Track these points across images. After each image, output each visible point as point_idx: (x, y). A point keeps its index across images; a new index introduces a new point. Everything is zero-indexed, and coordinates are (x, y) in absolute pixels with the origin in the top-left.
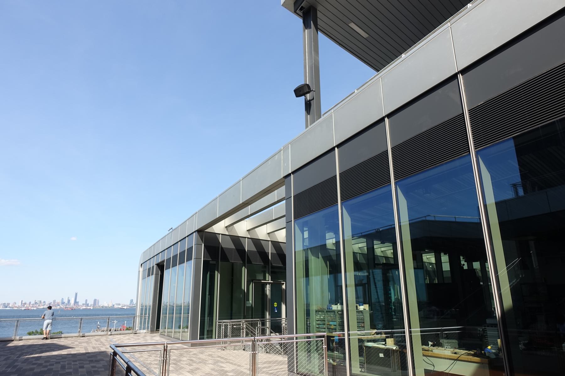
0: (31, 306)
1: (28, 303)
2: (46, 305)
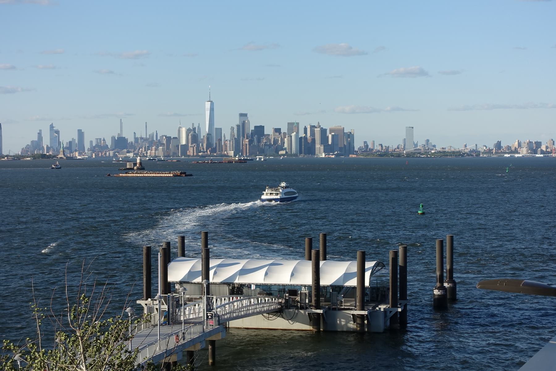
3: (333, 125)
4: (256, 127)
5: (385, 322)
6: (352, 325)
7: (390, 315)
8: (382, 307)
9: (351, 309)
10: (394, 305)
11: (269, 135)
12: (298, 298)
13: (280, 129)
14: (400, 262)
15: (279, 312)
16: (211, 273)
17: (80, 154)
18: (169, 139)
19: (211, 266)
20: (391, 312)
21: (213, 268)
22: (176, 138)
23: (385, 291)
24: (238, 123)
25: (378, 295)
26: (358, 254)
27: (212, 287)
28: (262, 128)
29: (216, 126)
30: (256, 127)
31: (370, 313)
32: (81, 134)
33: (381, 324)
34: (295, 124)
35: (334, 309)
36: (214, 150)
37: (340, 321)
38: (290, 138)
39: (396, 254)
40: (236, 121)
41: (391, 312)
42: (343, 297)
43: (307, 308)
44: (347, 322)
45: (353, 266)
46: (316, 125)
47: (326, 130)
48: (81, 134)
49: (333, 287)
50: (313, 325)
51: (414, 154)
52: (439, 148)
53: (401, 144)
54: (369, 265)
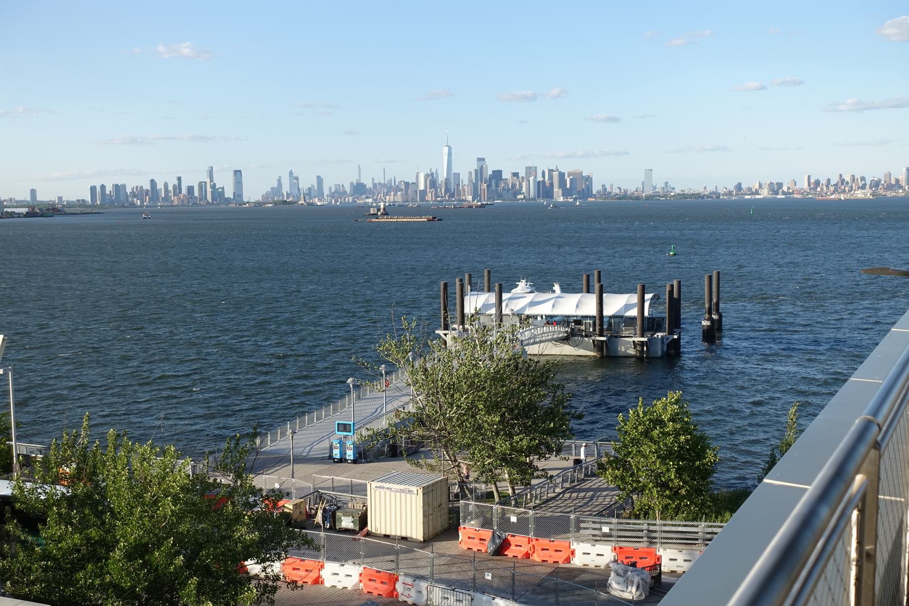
0: (832, 189)
1: (823, 181)
2: (868, 186)
3: (572, 169)
5: (662, 348)
6: (632, 352)
7: (666, 342)
8: (660, 334)
9: (632, 337)
10: (671, 333)
11: (507, 179)
12: (583, 328)
13: (518, 173)
14: (675, 295)
15: (565, 340)
16: (504, 304)
17: (320, 200)
18: (407, 184)
19: (503, 299)
20: (667, 339)
21: (505, 300)
23: (660, 321)
25: (653, 325)
26: (639, 287)
27: (504, 318)
28: (500, 172)
29: (454, 171)
31: (649, 340)
32: (320, 180)
33: (659, 351)
34: (533, 168)
35: (616, 337)
36: (452, 195)
37: (621, 348)
39: (672, 286)
40: (474, 166)
41: (667, 339)
42: (625, 326)
43: (591, 336)
44: (627, 349)
45: (634, 299)
46: (554, 168)
47: (564, 174)
48: (320, 180)
49: (614, 317)
50: (598, 351)
51: (654, 196)
52: (678, 191)
54: (648, 296)
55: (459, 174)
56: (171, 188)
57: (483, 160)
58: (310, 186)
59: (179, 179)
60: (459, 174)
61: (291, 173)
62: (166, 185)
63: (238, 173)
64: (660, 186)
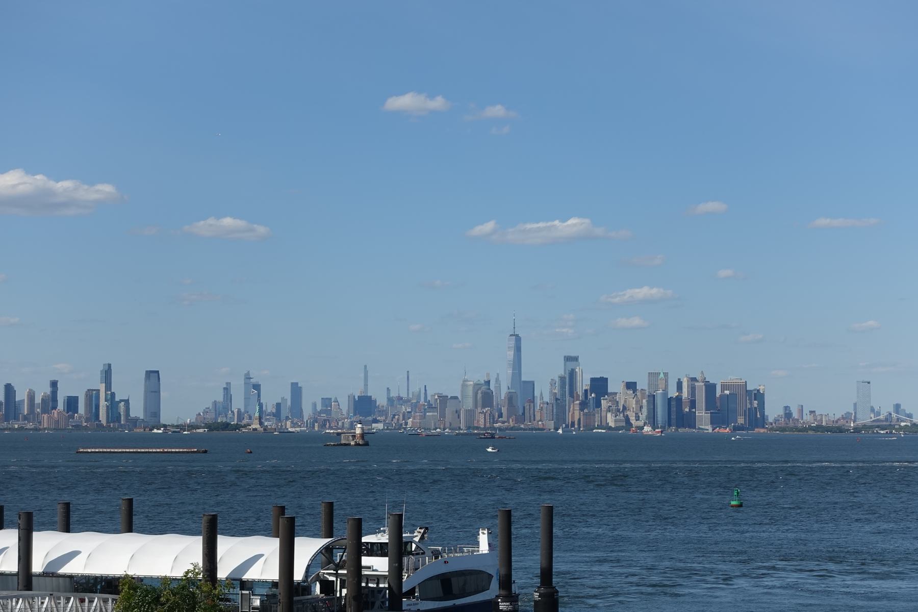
4: (593, 380)
11: (616, 394)
13: (635, 383)
17: (294, 425)
18: (443, 399)
22: (456, 398)
24: (562, 372)
29: (523, 379)
30: (593, 380)
32: (296, 390)
34: (662, 375)
38: (652, 399)
40: (559, 370)
46: (699, 377)
48: (296, 390)
51: (871, 427)
53: (850, 412)
55: (533, 383)
56: (38, 400)
57: (575, 359)
58: (280, 401)
59: (54, 384)
60: (533, 383)
61: (248, 377)
62: (31, 397)
63: (153, 376)
64: (886, 409)
